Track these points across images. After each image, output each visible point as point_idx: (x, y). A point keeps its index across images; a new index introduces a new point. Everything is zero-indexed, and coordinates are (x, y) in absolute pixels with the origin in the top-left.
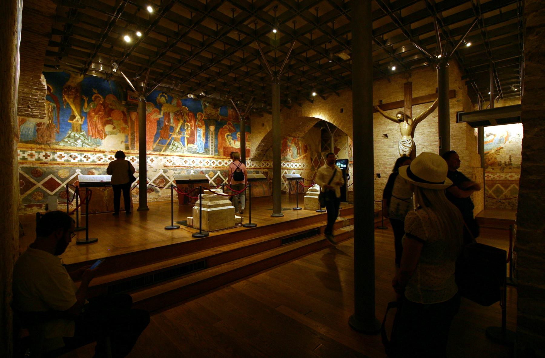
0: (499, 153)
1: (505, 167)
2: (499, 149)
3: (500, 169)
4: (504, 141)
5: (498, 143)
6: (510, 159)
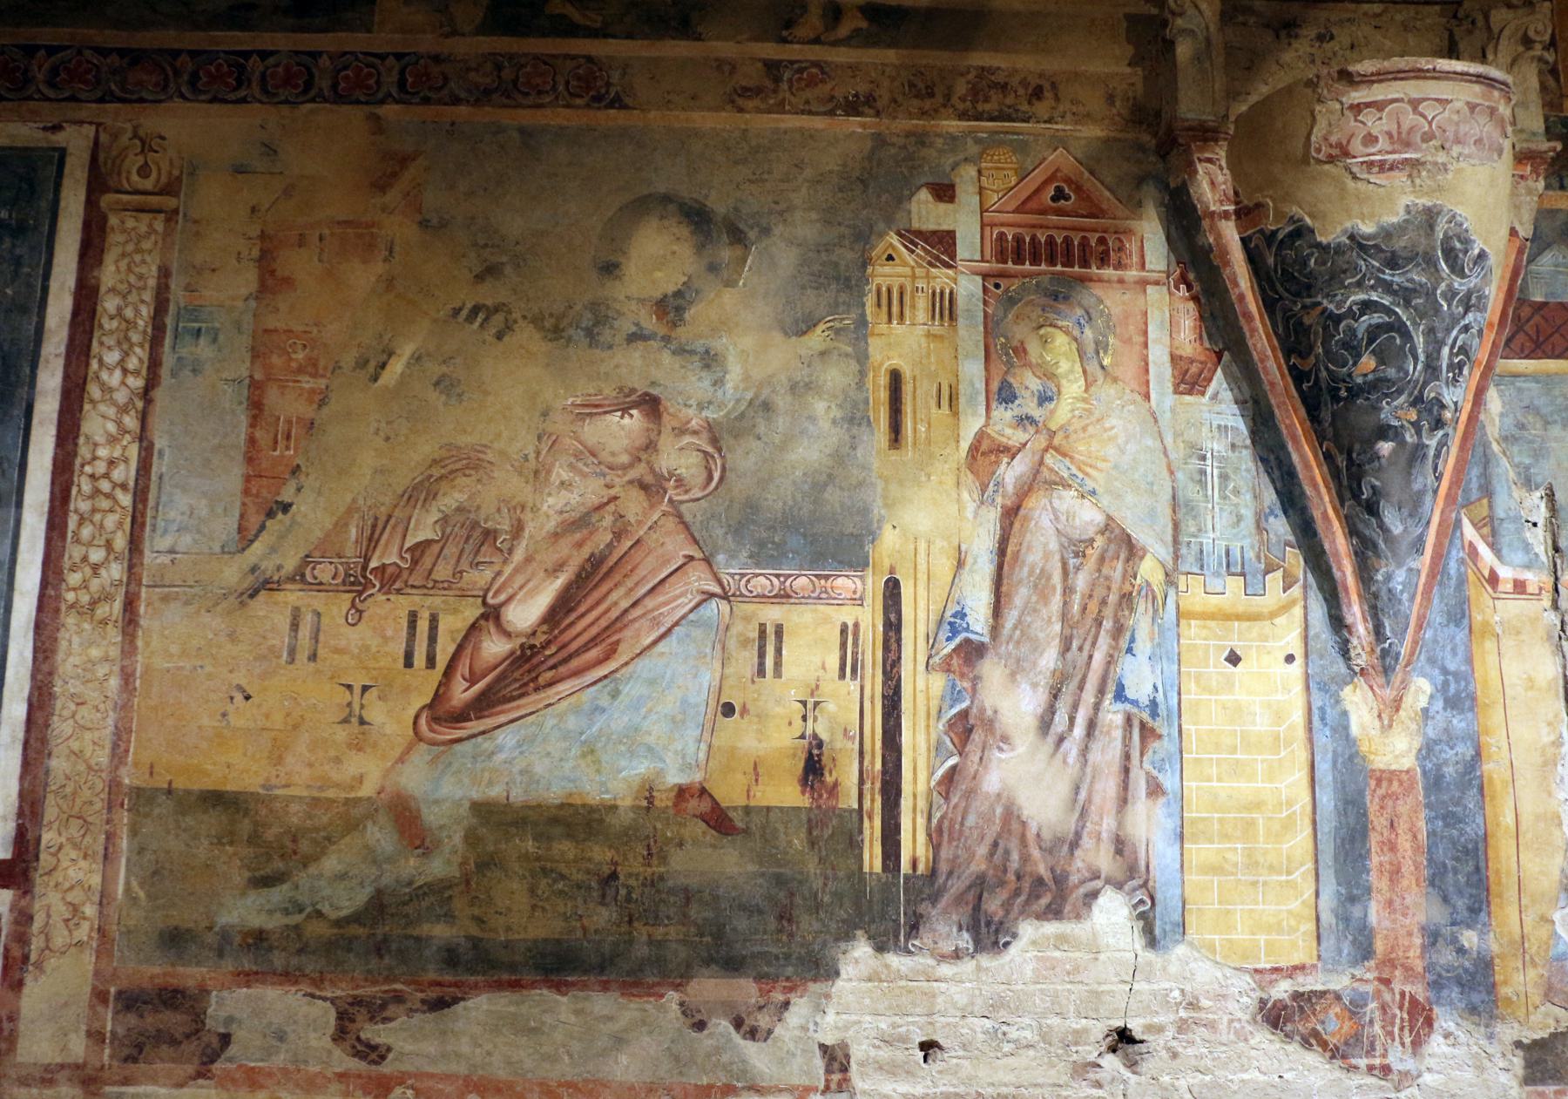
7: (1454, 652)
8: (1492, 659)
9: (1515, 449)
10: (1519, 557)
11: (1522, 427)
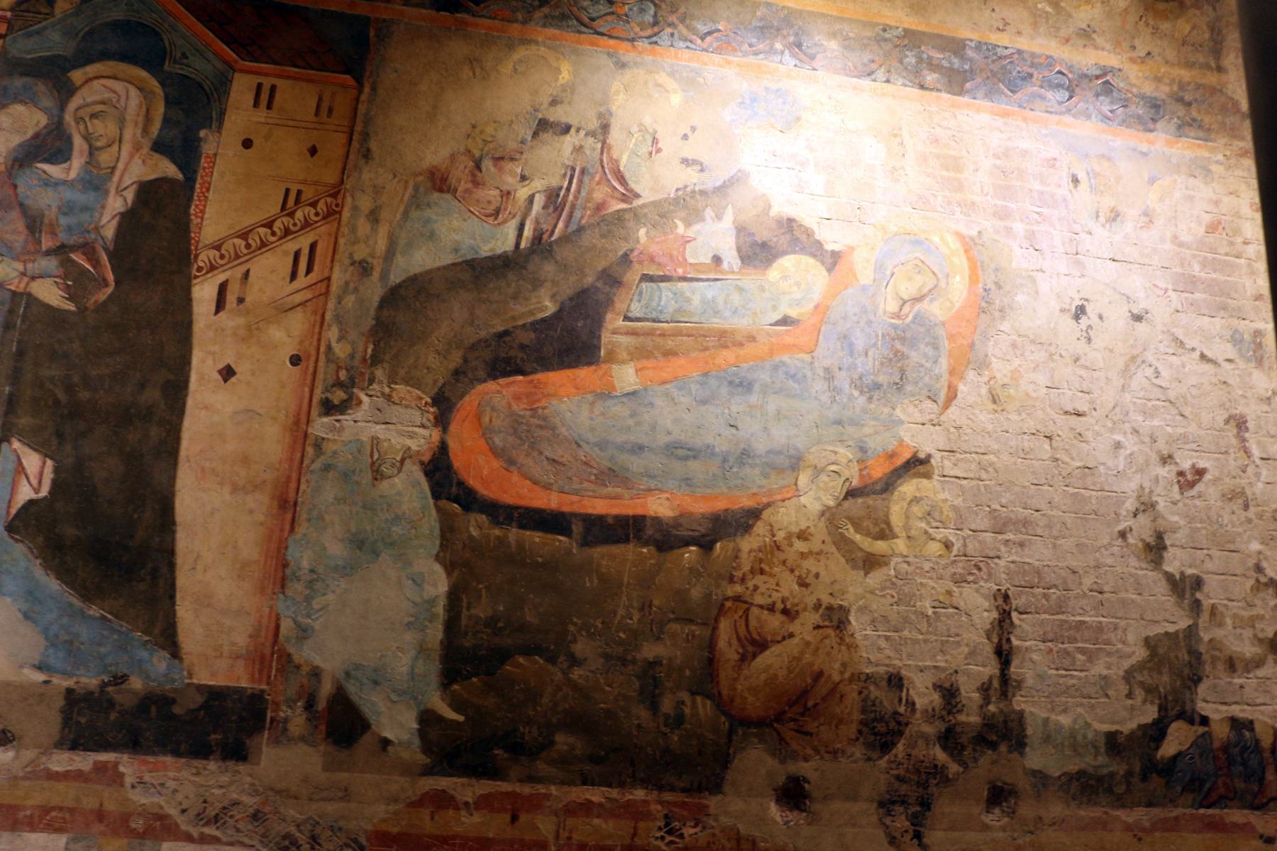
0: (885, 533)
1: (937, 771)
2: (879, 471)
3: (886, 804)
4: (944, 363)
5: (872, 389)
6: (1004, 655)
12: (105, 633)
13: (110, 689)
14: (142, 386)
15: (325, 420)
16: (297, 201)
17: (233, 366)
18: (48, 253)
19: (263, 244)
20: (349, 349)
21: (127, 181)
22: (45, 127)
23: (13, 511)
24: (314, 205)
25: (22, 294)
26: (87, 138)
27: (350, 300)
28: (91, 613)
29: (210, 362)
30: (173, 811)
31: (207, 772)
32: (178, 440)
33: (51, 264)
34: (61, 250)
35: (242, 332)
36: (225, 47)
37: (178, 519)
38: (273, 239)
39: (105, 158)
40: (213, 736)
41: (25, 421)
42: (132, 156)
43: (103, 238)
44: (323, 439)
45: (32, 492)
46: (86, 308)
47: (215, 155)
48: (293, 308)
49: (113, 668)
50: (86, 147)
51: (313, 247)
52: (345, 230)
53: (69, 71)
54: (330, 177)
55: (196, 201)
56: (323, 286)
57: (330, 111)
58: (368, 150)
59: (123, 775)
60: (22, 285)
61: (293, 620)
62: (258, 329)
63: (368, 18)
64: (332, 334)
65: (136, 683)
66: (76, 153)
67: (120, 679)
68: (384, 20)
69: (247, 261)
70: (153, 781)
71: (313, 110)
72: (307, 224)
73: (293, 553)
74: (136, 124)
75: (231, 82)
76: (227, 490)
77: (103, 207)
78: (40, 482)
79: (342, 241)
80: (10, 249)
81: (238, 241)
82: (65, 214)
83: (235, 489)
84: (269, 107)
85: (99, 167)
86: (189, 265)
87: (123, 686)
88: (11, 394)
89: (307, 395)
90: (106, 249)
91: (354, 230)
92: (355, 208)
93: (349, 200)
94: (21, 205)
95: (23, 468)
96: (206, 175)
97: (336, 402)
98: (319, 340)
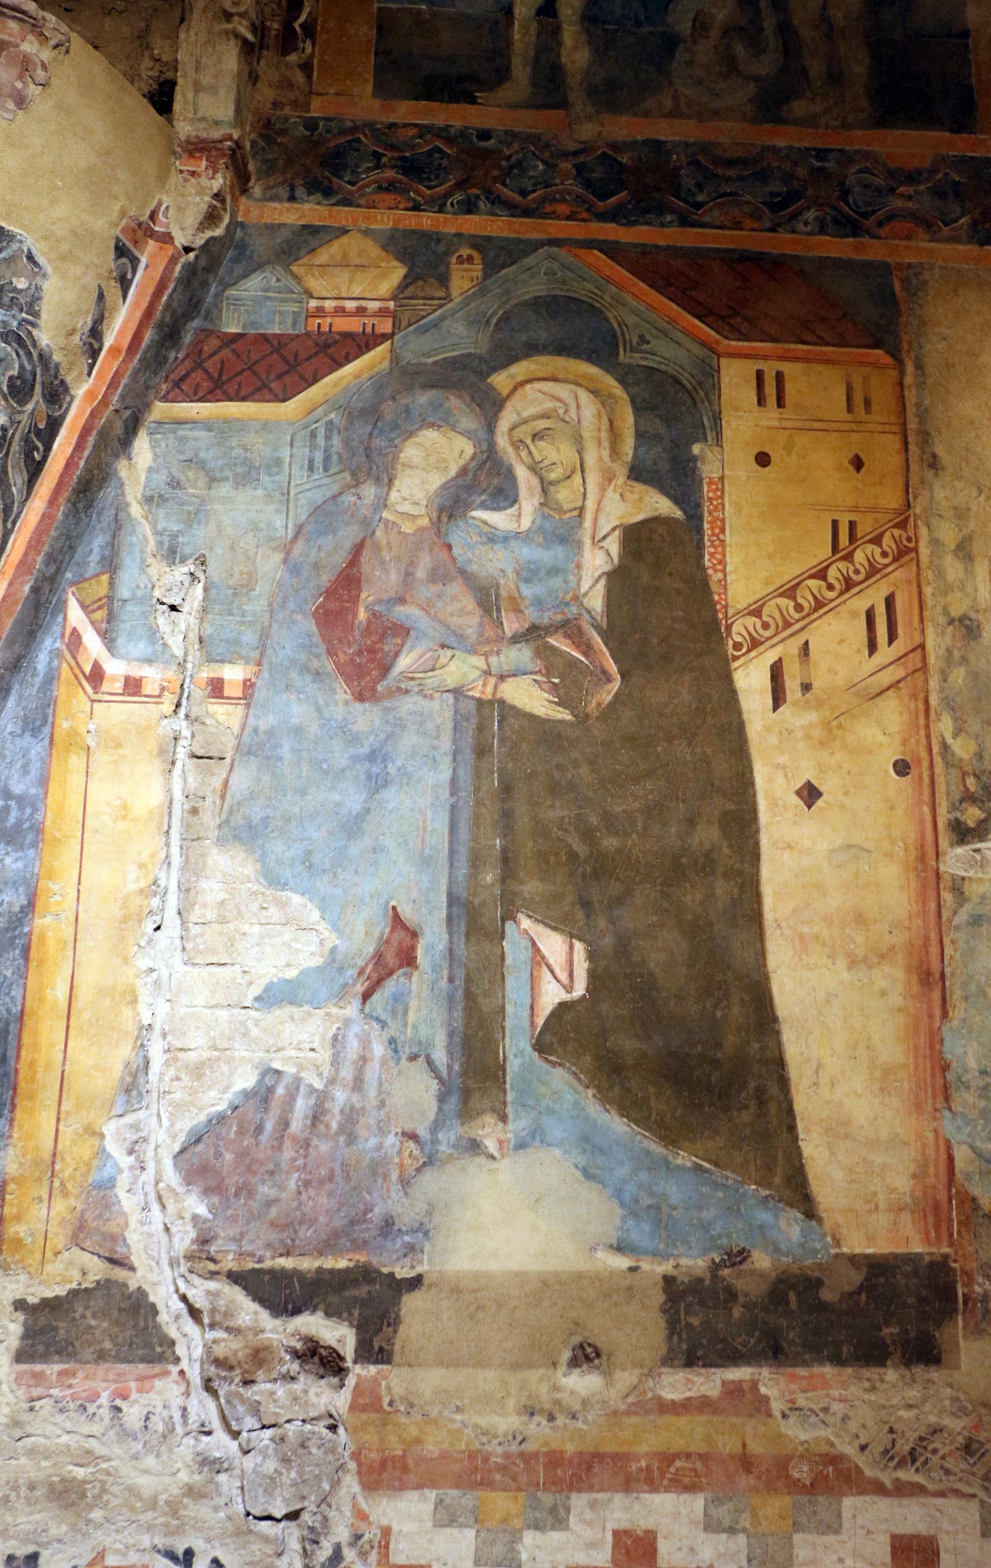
7: (25, 770)
8: (76, 780)
9: (161, 513)
10: (141, 648)
11: (175, 484)
12: (704, 1190)
13: (726, 1272)
14: (691, 822)
15: (960, 850)
16: (852, 538)
17: (815, 782)
18: (515, 640)
19: (819, 604)
20: (973, 747)
21: (605, 528)
22: (473, 458)
23: (540, 1022)
24: (877, 541)
25: (491, 702)
26: (534, 468)
27: (959, 676)
28: (679, 1161)
29: (780, 779)
30: (848, 1449)
31: (885, 1386)
32: (758, 897)
33: (522, 655)
34: (533, 633)
35: (817, 733)
36: (697, 322)
37: (781, 1012)
38: (832, 595)
39: (564, 495)
40: (886, 1331)
41: (531, 887)
42: (603, 491)
43: (589, 612)
44: (963, 879)
45: (563, 991)
46: (587, 716)
47: (722, 478)
48: (882, 692)
49: (725, 1241)
50: (535, 481)
51: (890, 602)
52: (929, 575)
53: (489, 375)
54: (891, 499)
55: (708, 550)
56: (918, 654)
57: (867, 403)
58: (934, 456)
59: (766, 1399)
60: (489, 690)
61: (971, 1147)
62: (840, 726)
63: (886, 265)
64: (944, 726)
65: (762, 1261)
66: (523, 492)
67: (738, 1257)
68: (910, 266)
69: (802, 629)
70: (814, 1407)
71: (843, 404)
72: (873, 570)
73: (953, 1048)
74: (599, 442)
75: (719, 371)
76: (842, 964)
77: (579, 566)
78: (571, 975)
79: (928, 591)
80: (461, 637)
81: (783, 602)
82: (527, 581)
83: (853, 963)
84: (780, 403)
85: (559, 510)
86: (721, 641)
87: (744, 1267)
88: (505, 850)
89: (928, 817)
90: (597, 627)
91: (940, 574)
92: (935, 542)
93: (923, 531)
94: (462, 572)
95: (543, 957)
96: (716, 508)
97: (971, 824)
98: (928, 736)
